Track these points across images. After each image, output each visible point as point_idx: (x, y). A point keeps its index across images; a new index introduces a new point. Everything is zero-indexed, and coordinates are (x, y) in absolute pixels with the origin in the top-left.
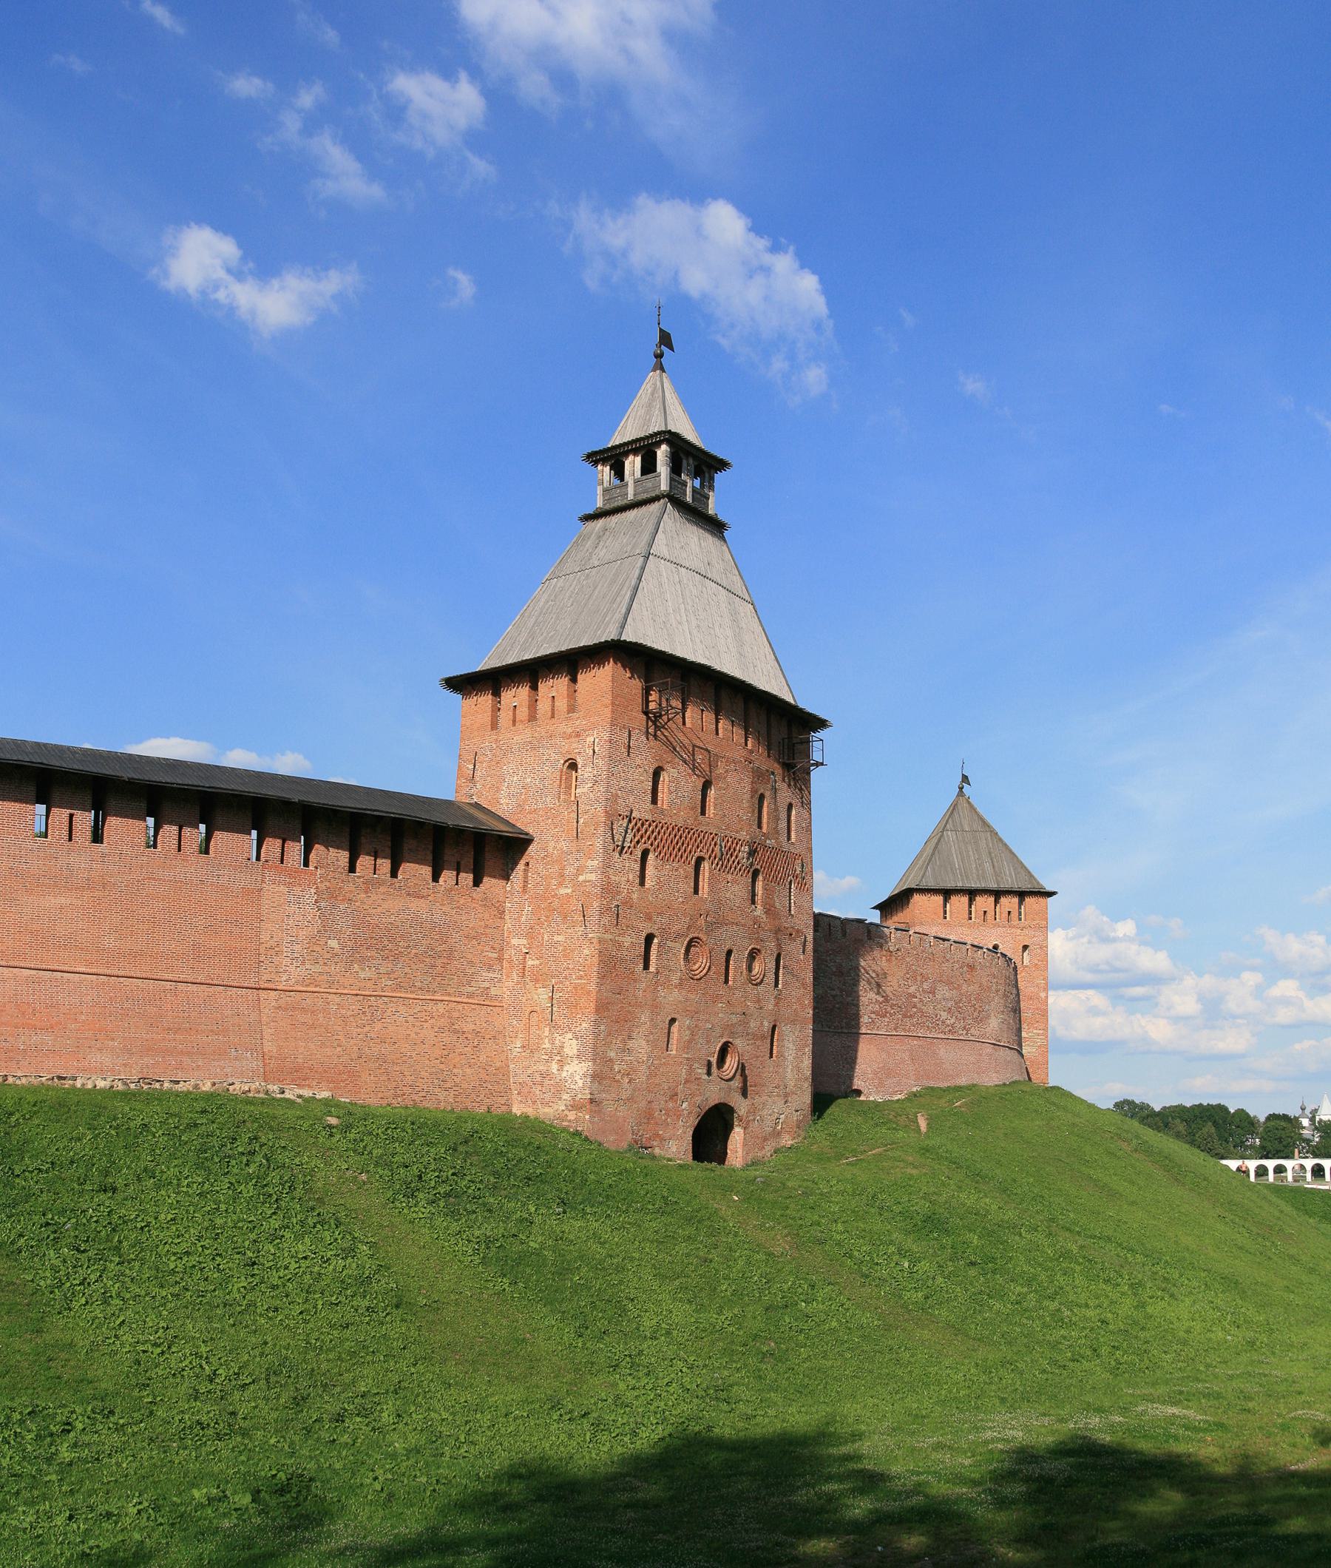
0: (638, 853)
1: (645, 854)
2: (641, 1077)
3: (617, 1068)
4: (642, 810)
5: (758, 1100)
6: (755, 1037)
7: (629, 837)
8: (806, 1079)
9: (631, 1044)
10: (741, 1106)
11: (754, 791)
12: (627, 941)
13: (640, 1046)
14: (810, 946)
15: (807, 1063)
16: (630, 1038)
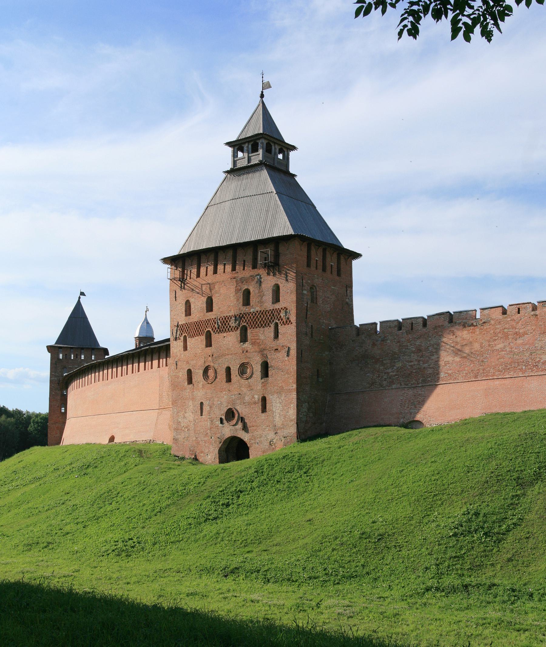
0: (182, 338)
4: (183, 320)
5: (256, 433)
6: (249, 404)
8: (292, 421)
10: (245, 437)
11: (237, 291)
12: (180, 374)
14: (293, 352)
15: (292, 413)
16: (185, 413)
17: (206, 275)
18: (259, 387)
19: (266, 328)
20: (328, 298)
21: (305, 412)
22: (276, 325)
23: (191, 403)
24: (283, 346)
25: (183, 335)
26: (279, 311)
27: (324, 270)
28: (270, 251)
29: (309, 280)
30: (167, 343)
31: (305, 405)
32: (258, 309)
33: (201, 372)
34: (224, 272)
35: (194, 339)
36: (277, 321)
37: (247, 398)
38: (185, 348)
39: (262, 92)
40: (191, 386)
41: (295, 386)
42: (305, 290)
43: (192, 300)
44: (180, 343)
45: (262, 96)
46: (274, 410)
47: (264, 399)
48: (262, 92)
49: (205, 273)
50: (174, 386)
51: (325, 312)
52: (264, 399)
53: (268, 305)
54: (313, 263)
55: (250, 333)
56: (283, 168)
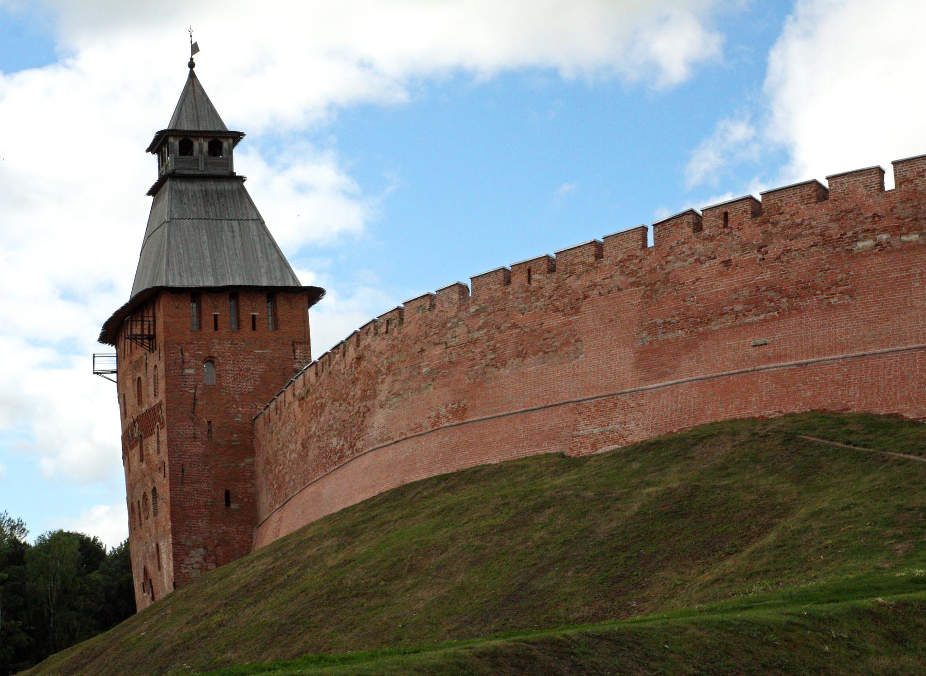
20: (248, 370)
21: (197, 562)
29: (199, 350)
39: (192, 59)
42: (190, 367)
45: (191, 65)
48: (192, 59)
51: (242, 394)
56: (220, 171)
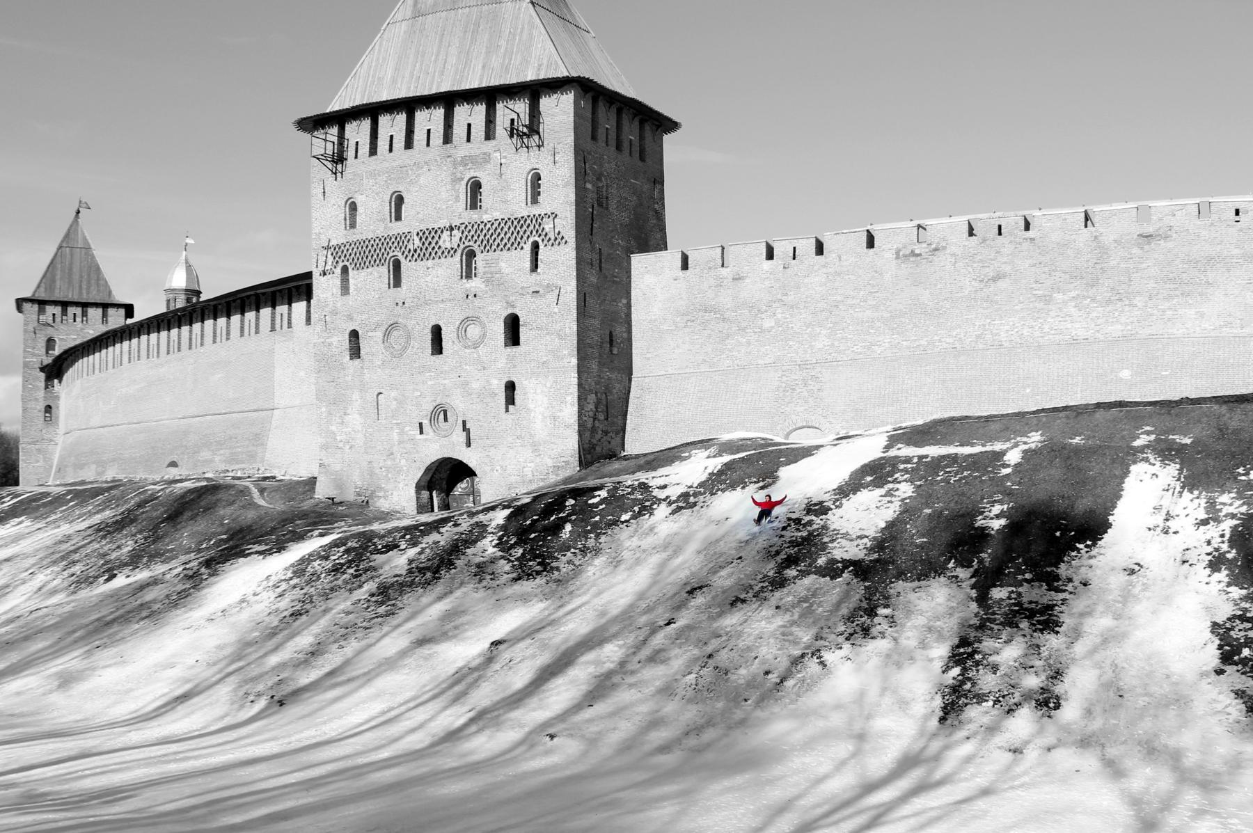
0: (338, 271)
1: (345, 270)
2: (360, 440)
3: (339, 438)
7: (330, 262)
9: (347, 418)
12: (335, 340)
13: (355, 419)
17: (391, 150)
18: (501, 363)
19: (513, 252)
22: (536, 246)
23: (356, 396)
24: (548, 286)
25: (341, 264)
26: (539, 219)
27: (619, 147)
28: (521, 107)
30: (307, 282)
31: (592, 398)
32: (498, 215)
33: (379, 334)
34: (428, 145)
35: (363, 273)
36: (536, 238)
37: (475, 385)
38: (345, 289)
40: (357, 362)
41: (574, 361)
43: (359, 200)
44: (335, 280)
46: (531, 406)
47: (511, 387)
49: (387, 147)
50: (324, 363)
52: (511, 387)
53: (518, 206)
54: (601, 133)
55: (480, 259)
